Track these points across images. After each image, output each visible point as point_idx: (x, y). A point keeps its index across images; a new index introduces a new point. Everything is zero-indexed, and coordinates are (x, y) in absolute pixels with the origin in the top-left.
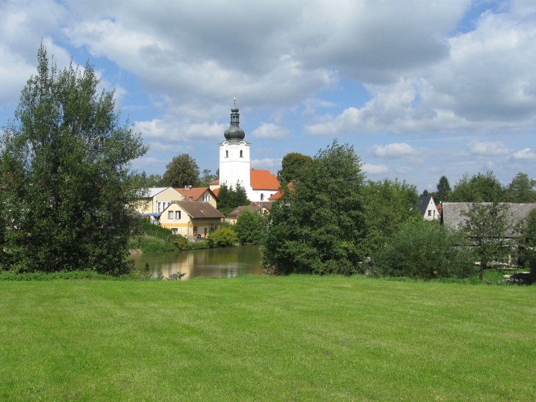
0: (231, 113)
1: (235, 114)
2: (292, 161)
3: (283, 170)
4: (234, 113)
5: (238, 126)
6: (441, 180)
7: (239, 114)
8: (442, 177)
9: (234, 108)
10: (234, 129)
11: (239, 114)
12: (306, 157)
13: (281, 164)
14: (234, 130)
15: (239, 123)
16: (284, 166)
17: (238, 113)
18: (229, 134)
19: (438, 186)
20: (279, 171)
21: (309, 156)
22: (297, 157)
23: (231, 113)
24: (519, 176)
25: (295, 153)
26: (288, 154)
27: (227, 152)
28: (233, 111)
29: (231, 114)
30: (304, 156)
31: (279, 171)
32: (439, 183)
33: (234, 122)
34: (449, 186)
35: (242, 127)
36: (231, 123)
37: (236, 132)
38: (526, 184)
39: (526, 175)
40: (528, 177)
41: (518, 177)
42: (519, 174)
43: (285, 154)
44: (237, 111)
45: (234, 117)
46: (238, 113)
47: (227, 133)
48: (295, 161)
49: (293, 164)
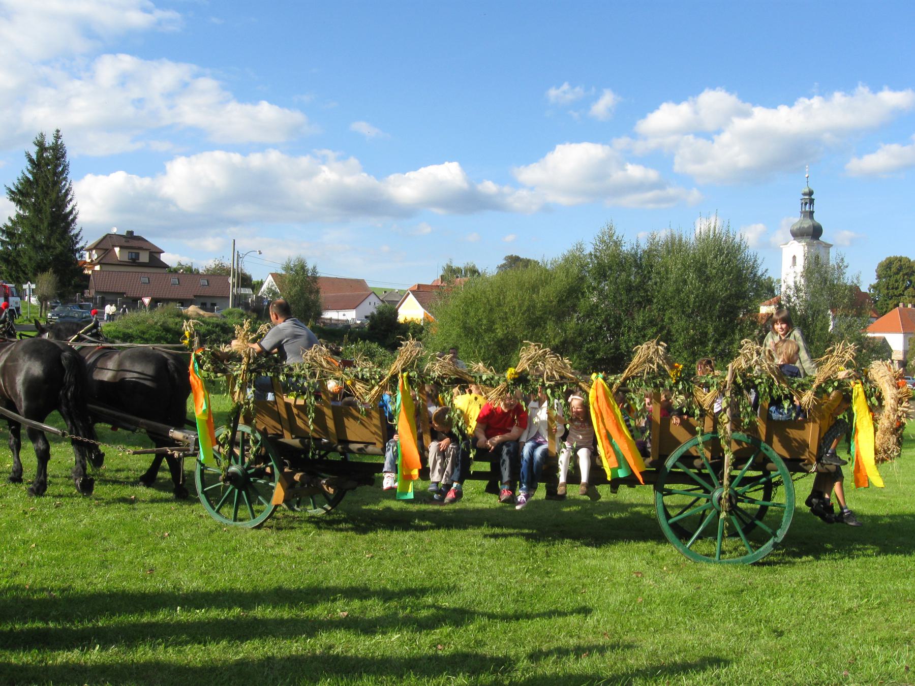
1: (809, 198)
2: (894, 269)
3: (878, 284)
9: (807, 190)
13: (874, 275)
14: (806, 226)
15: (813, 212)
16: (879, 277)
20: (870, 285)
22: (902, 263)
25: (899, 256)
26: (887, 259)
27: (794, 257)
28: (805, 194)
31: (870, 285)
33: (807, 212)
35: (818, 218)
36: (801, 213)
37: (809, 228)
43: (882, 258)
44: (811, 193)
45: (806, 204)
47: (795, 228)
48: (900, 269)
49: (897, 273)
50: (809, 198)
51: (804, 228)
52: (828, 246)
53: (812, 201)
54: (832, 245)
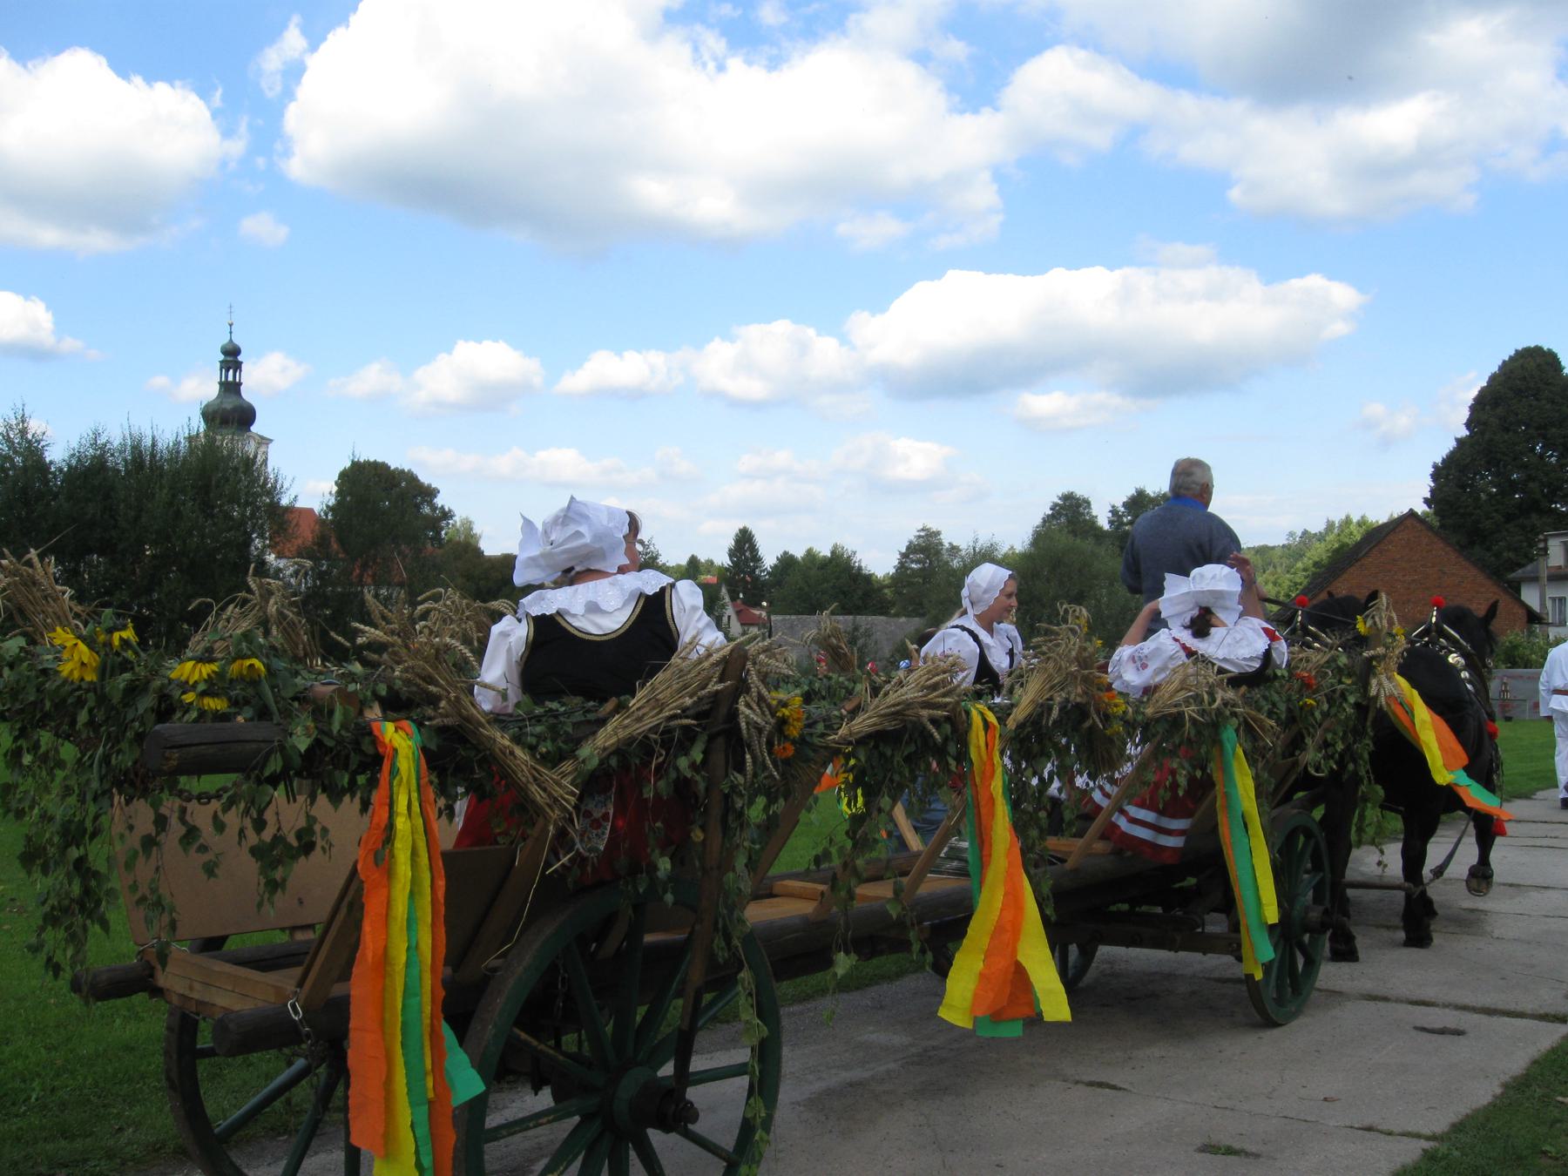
0: (222, 357)
1: (232, 358)
4: (229, 359)
5: (238, 392)
6: (737, 535)
7: (241, 363)
8: (740, 531)
9: (230, 347)
10: (230, 400)
11: (241, 363)
12: (403, 471)
14: (229, 404)
15: (240, 384)
17: (240, 358)
18: (215, 412)
19: (730, 550)
21: (409, 471)
23: (222, 357)
24: (922, 534)
29: (221, 362)
30: (397, 469)
32: (733, 543)
34: (757, 550)
35: (247, 394)
36: (221, 384)
37: (235, 410)
38: (938, 553)
39: (938, 533)
40: (942, 537)
41: (920, 537)
42: (923, 530)
45: (227, 371)
46: (240, 358)
50: (232, 358)
51: (224, 410)
52: (264, 441)
53: (237, 366)
54: (271, 441)
